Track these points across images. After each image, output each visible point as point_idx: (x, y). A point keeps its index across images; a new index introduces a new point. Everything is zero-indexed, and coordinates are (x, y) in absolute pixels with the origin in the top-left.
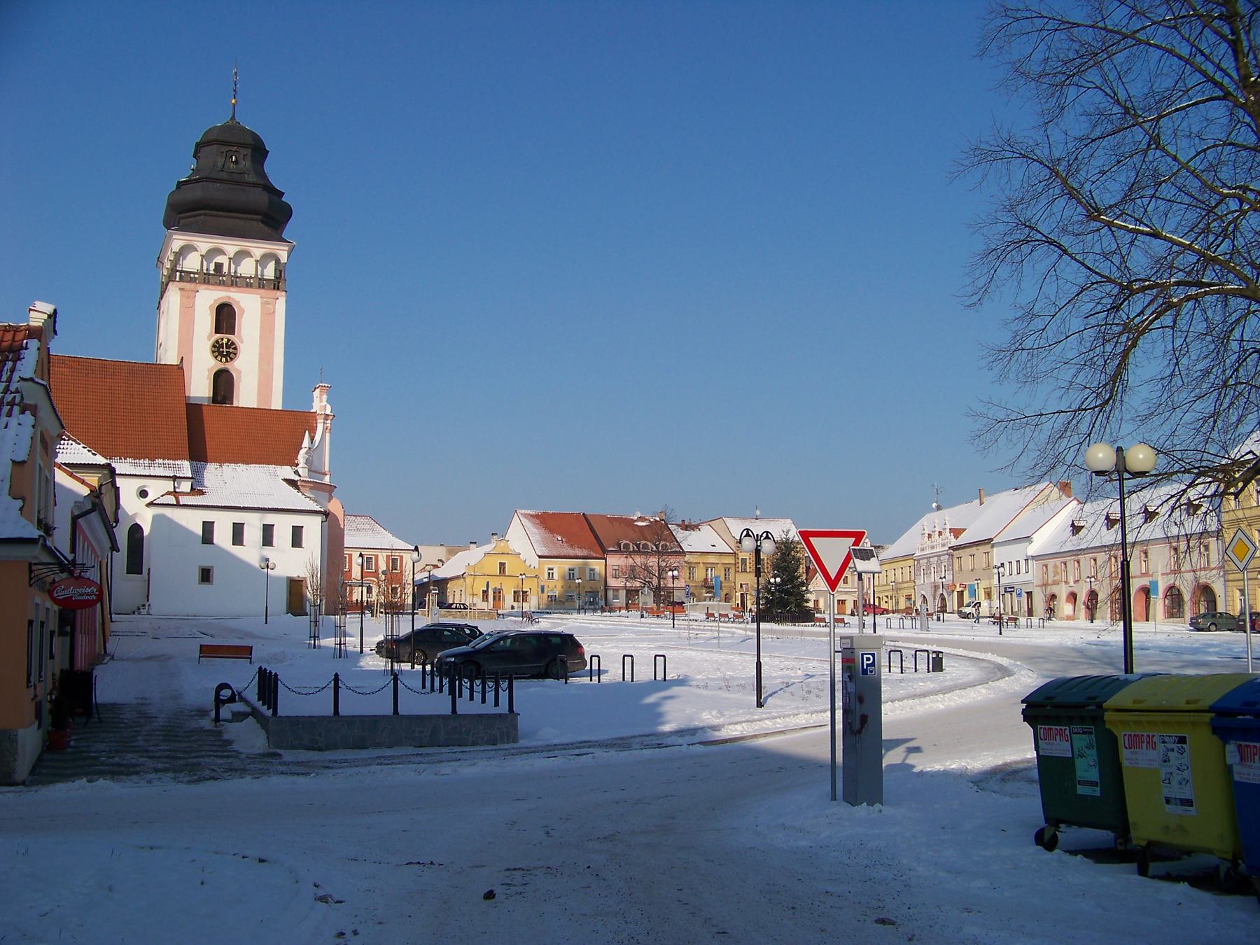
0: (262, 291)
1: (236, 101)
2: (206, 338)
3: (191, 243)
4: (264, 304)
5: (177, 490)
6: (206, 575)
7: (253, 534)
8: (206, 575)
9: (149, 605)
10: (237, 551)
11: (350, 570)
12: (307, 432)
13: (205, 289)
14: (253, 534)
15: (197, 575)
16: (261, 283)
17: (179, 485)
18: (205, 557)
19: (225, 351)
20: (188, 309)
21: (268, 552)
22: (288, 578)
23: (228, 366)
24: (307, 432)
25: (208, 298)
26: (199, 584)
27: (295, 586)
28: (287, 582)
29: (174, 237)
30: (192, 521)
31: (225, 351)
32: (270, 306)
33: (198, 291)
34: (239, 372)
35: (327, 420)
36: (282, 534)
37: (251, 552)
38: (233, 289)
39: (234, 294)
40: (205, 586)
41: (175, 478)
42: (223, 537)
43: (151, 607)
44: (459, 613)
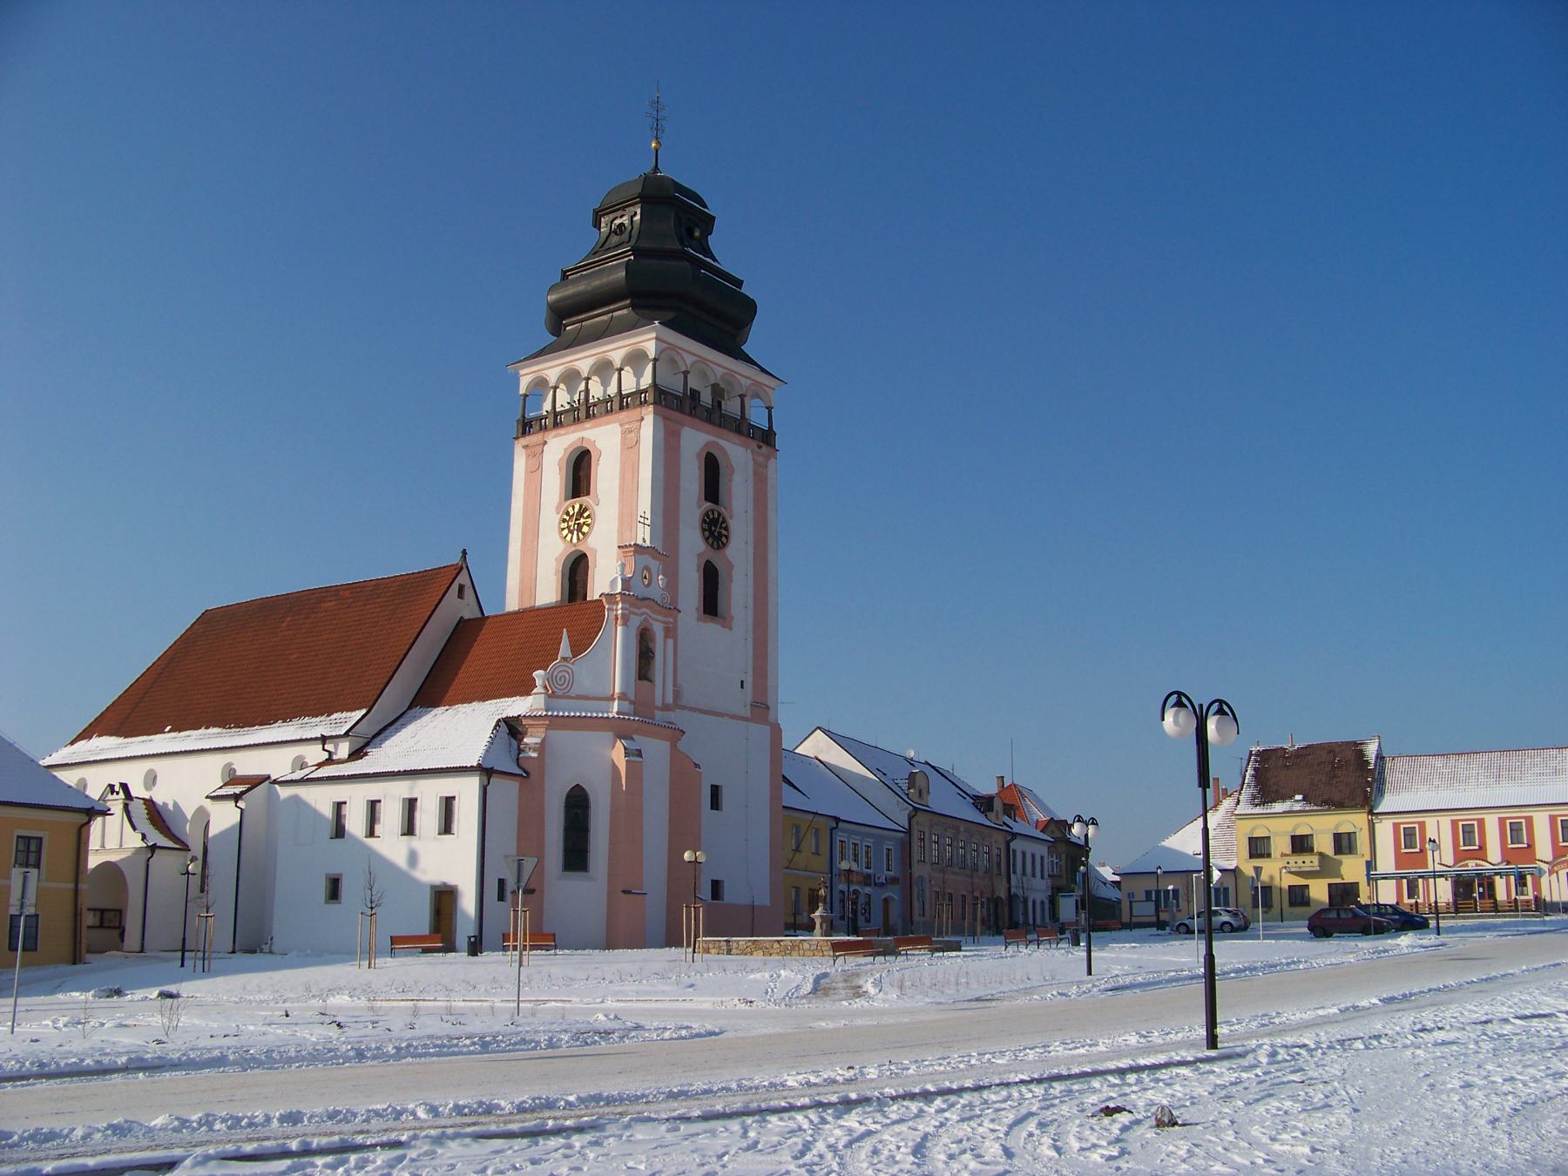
0: (623, 415)
1: (658, 143)
2: (554, 513)
3: (540, 374)
4: (623, 433)
5: (335, 757)
6: (334, 889)
7: (391, 816)
8: (334, 889)
9: (272, 939)
10: (370, 841)
11: (1530, 846)
12: (565, 630)
13: (555, 436)
14: (391, 816)
15: (321, 889)
16: (623, 402)
17: (336, 748)
18: (333, 858)
19: (578, 522)
20: (535, 469)
21: (413, 842)
22: (433, 887)
23: (582, 548)
24: (565, 630)
25: (558, 447)
26: (326, 902)
27: (444, 897)
28: (431, 893)
29: (522, 372)
30: (321, 799)
31: (578, 522)
32: (633, 435)
33: (545, 443)
34: (595, 552)
35: (617, 603)
36: (427, 818)
37: (390, 845)
38: (588, 425)
39: (589, 431)
40: (334, 907)
41: (324, 739)
42: (355, 823)
43: (274, 939)
44: (776, 945)
